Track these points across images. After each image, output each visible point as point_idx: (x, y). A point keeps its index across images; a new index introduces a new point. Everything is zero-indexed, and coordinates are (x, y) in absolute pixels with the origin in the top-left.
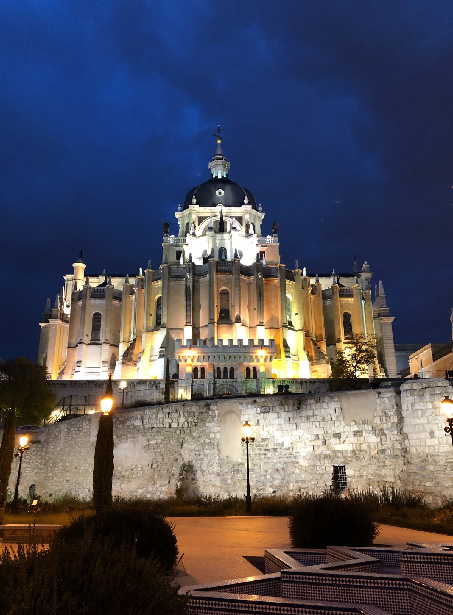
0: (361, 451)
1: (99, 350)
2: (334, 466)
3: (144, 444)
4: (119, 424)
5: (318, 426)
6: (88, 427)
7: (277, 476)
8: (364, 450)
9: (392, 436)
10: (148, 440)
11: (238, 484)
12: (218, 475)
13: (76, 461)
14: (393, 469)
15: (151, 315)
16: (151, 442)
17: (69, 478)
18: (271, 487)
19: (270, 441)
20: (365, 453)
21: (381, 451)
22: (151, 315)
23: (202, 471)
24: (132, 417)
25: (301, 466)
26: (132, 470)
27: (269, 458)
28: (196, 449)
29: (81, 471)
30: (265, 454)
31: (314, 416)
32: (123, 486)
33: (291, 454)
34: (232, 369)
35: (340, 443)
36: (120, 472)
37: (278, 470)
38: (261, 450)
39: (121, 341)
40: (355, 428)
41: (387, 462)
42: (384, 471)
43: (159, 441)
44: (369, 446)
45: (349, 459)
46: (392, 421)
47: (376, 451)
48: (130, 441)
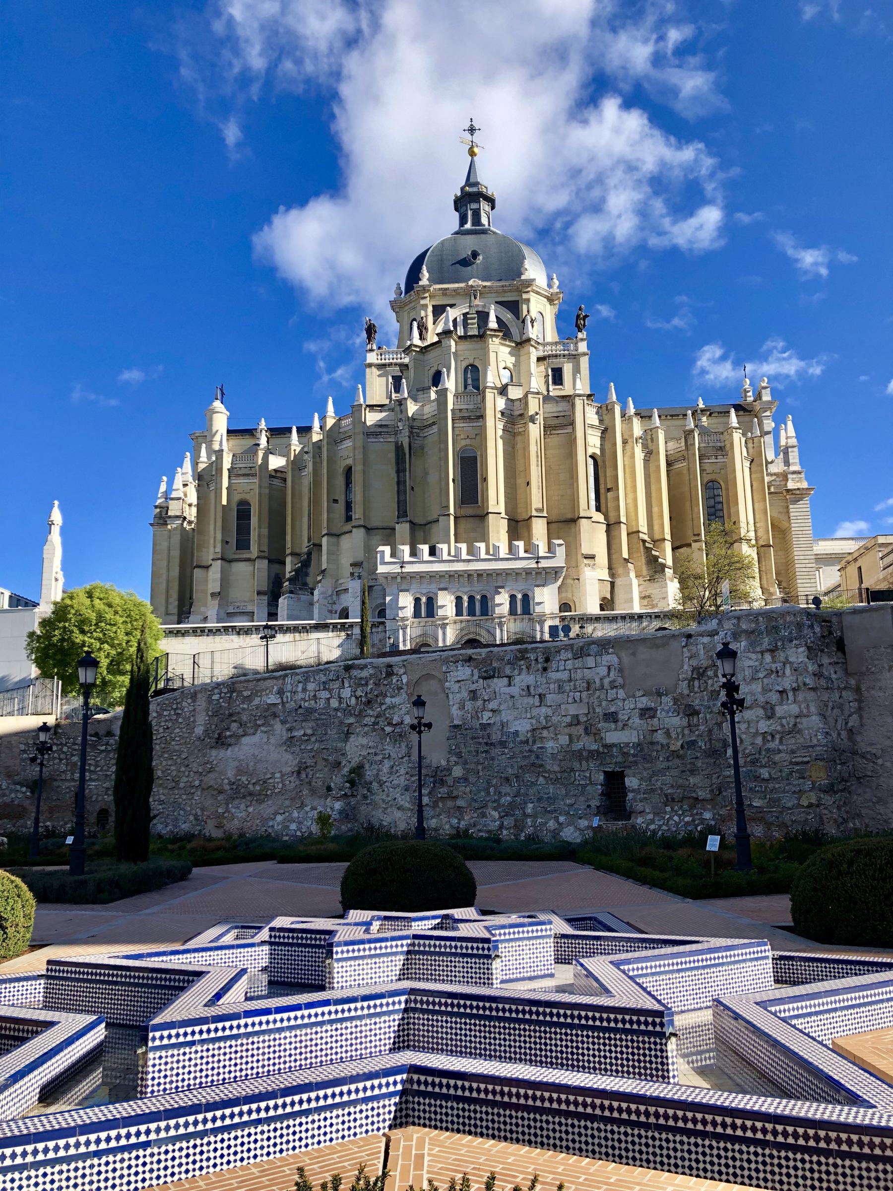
0: (652, 743)
1: (251, 568)
2: (605, 772)
3: (286, 735)
4: (243, 703)
5: (577, 699)
6: (191, 708)
7: (505, 789)
8: (658, 743)
9: (708, 716)
10: (290, 730)
11: (440, 805)
12: (406, 790)
13: (173, 768)
14: (709, 776)
15: (336, 501)
16: (296, 734)
17: (163, 798)
18: (495, 809)
19: (495, 728)
20: (659, 747)
21: (687, 743)
22: (336, 501)
23: (381, 784)
24: (263, 690)
25: (549, 772)
26: (265, 782)
27: (493, 759)
28: (370, 744)
29: (182, 785)
30: (486, 752)
31: (570, 680)
32: (251, 809)
33: (530, 751)
34: (484, 598)
35: (616, 729)
36: (246, 787)
37: (507, 780)
38: (480, 743)
39: (288, 551)
40: (644, 702)
41: (699, 763)
42: (692, 780)
43: (309, 732)
44: (668, 733)
45: (631, 759)
46: (710, 688)
47: (679, 743)
48: (262, 732)
